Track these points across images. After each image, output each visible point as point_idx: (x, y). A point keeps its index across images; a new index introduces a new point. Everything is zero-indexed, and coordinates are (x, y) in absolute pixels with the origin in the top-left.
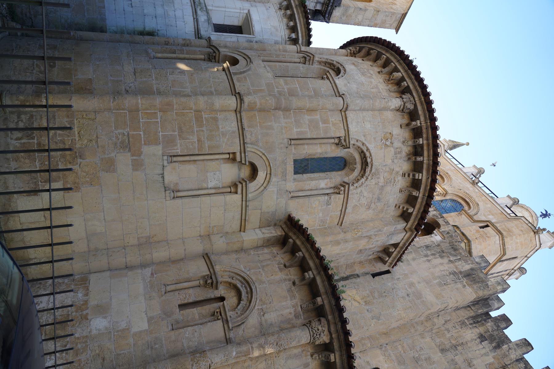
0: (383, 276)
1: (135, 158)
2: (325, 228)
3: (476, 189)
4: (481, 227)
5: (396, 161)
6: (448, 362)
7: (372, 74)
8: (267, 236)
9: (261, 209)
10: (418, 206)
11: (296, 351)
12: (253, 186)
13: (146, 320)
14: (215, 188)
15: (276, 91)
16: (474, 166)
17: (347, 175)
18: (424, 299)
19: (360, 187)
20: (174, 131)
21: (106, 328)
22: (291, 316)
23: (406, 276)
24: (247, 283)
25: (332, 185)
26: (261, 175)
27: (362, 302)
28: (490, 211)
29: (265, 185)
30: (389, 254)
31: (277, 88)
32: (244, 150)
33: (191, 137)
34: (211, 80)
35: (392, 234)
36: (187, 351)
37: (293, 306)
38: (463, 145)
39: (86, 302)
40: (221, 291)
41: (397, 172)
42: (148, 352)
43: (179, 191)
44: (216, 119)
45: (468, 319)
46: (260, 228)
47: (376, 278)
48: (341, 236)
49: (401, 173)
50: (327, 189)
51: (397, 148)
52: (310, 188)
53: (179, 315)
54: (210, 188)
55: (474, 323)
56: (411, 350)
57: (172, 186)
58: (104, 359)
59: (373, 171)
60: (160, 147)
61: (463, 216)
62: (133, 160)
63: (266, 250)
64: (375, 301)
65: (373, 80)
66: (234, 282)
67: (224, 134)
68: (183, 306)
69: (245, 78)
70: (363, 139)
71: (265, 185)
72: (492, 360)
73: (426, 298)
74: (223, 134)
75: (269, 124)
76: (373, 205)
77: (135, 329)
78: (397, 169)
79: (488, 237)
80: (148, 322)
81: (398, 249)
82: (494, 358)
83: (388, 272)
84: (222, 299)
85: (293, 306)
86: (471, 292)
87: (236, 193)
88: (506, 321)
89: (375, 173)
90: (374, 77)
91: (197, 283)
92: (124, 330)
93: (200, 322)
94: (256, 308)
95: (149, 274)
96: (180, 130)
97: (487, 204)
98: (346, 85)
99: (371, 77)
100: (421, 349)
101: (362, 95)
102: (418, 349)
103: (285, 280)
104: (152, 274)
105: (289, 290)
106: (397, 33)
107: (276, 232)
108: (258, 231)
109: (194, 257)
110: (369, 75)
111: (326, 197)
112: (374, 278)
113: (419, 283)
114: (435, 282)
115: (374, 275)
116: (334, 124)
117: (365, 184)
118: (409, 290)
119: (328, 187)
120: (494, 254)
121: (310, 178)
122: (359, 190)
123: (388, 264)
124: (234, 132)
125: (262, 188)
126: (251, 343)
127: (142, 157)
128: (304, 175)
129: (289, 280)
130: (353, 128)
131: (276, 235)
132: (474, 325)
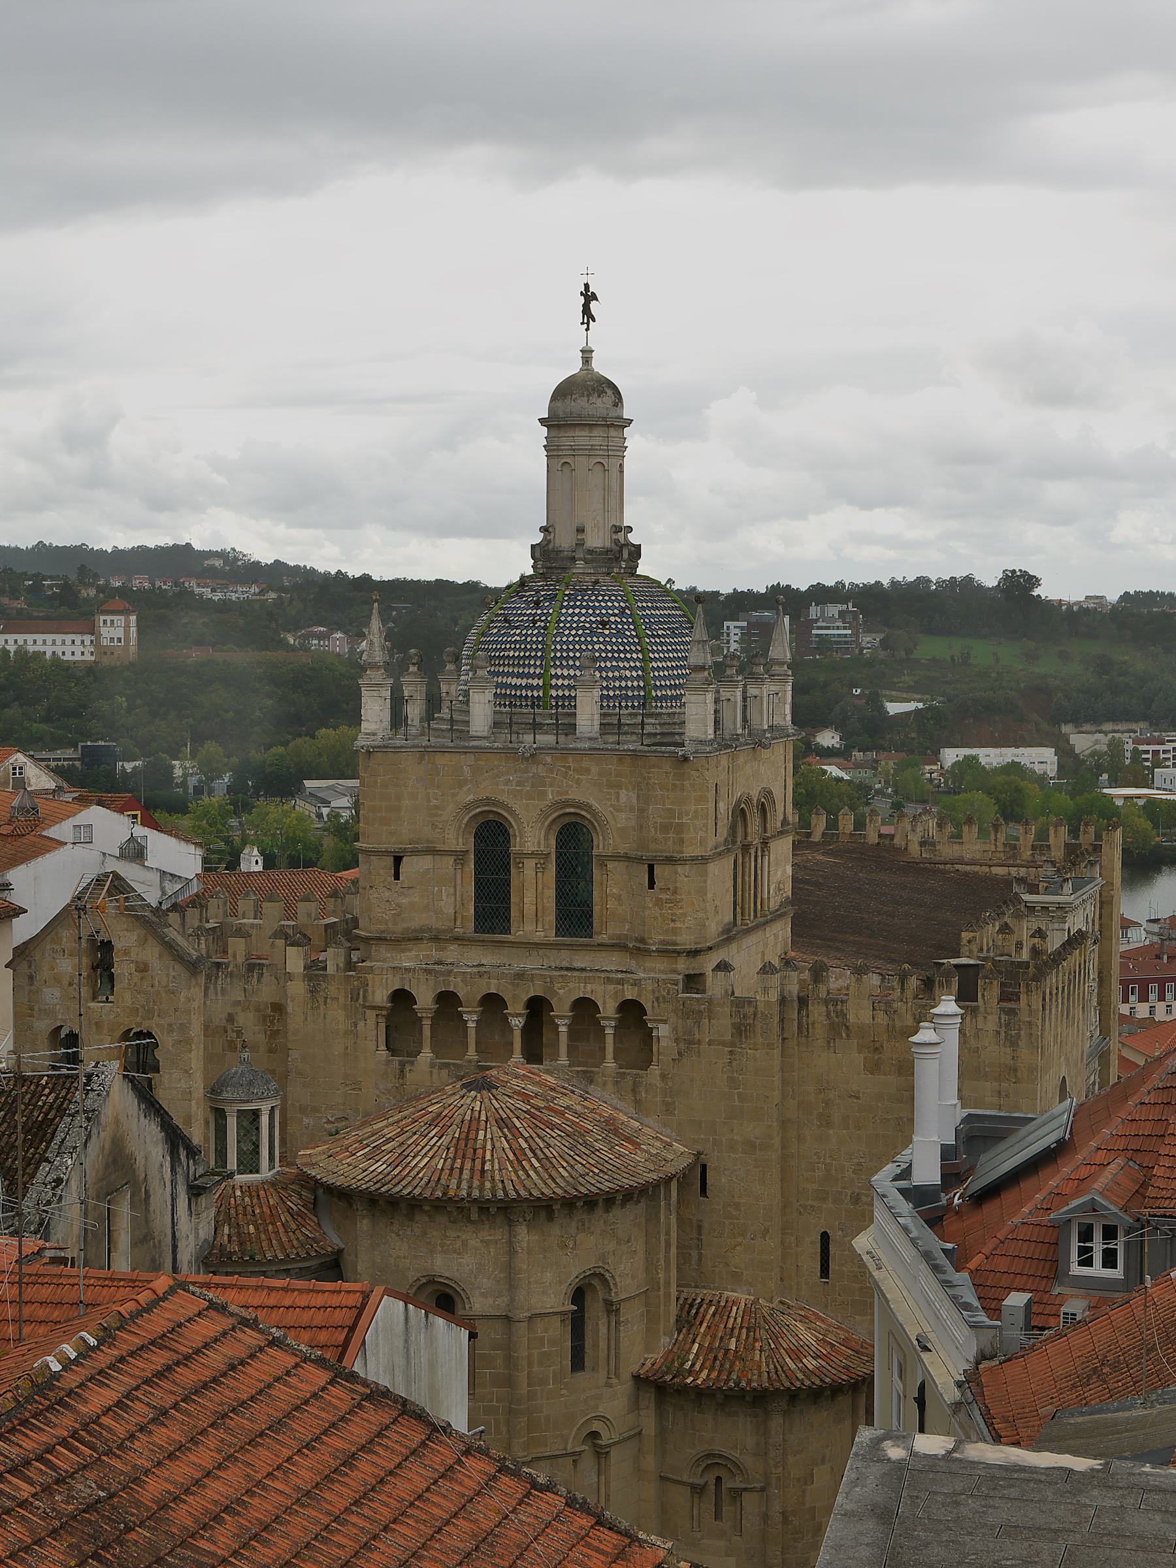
3: (542, 756)
4: (651, 884)
7: (458, 1237)
8: (652, 1405)
26: (596, 1426)
31: (492, 1401)
32: (573, 1454)
40: (711, 1478)
45: (799, 1044)
48: (661, 1293)
50: (609, 1322)
52: (606, 1347)
55: (807, 1037)
61: (610, 865)
66: (704, 1465)
68: (718, 1516)
70: (564, 1287)
73: (757, 1138)
86: (767, 1054)
93: (739, 1509)
94: (738, 1456)
97: (588, 771)
99: (465, 1243)
101: (502, 1275)
110: (459, 1243)
111: (622, 1328)
125: (607, 1422)
128: (587, 1351)
129: (717, 1410)
131: (653, 1395)
132: (810, 1039)
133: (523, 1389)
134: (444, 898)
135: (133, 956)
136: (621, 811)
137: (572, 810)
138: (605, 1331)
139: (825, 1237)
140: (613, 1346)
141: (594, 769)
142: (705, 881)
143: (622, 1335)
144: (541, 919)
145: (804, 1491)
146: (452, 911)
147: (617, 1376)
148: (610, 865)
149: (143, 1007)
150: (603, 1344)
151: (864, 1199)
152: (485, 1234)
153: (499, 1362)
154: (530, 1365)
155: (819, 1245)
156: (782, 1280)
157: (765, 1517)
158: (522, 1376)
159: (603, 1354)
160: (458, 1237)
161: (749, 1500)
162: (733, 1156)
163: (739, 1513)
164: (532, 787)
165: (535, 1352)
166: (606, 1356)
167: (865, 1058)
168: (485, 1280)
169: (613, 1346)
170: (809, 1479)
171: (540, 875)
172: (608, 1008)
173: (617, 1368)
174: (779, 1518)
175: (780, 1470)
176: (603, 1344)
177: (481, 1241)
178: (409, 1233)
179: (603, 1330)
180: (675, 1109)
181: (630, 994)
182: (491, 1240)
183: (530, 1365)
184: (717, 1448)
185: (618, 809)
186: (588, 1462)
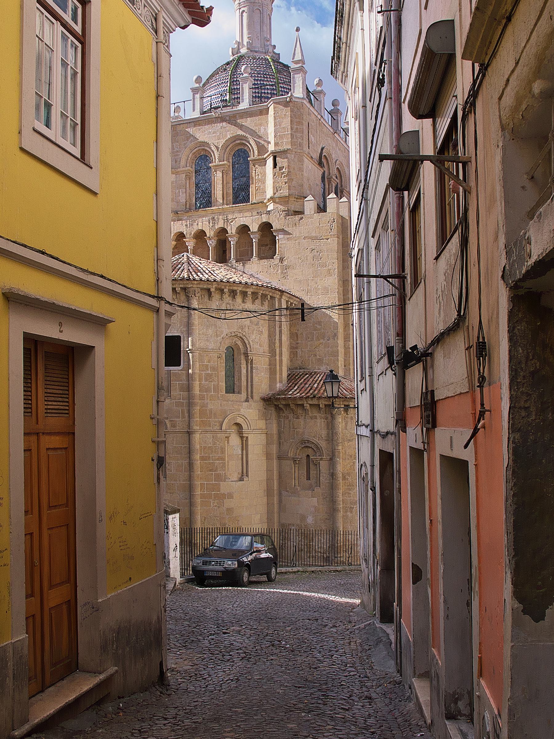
2: (270, 369)
9: (257, 420)
12: (244, 426)
14: (242, 450)
15: (183, 401)
17: (239, 349)
19: (249, 342)
21: (313, 517)
22: (326, 422)
24: (303, 442)
25: (245, 362)
26: (239, 421)
27: (322, 341)
29: (244, 418)
36: (331, 481)
42: (328, 499)
43: (242, 472)
48: (277, 358)
50: (247, 367)
53: (312, 481)
54: (242, 452)
59: (240, 331)
63: (282, 420)
67: (214, 443)
68: (308, 478)
71: (244, 418)
84: (308, 456)
87: (247, 437)
89: (242, 329)
91: (297, 468)
93: (318, 472)
96: (211, 470)
101: (185, 329)
103: (305, 418)
107: (272, 411)
109: (280, 466)
111: (254, 371)
112: (305, 321)
116: (209, 362)
117: (248, 337)
121: (239, 380)
122: (251, 342)
124: (213, 437)
125: (246, 420)
127: (226, 493)
130: (211, 346)
137: (239, 142)
138: (245, 372)
140: (249, 380)
142: (302, 164)
144: (225, 198)
147: (252, 398)
150: (244, 379)
156: (345, 366)
158: (196, 385)
159: (244, 383)
161: (324, 465)
163: (318, 473)
169: (249, 380)
172: (254, 228)
173: (252, 392)
176: (244, 379)
179: (244, 371)
184: (306, 437)
186: (235, 440)
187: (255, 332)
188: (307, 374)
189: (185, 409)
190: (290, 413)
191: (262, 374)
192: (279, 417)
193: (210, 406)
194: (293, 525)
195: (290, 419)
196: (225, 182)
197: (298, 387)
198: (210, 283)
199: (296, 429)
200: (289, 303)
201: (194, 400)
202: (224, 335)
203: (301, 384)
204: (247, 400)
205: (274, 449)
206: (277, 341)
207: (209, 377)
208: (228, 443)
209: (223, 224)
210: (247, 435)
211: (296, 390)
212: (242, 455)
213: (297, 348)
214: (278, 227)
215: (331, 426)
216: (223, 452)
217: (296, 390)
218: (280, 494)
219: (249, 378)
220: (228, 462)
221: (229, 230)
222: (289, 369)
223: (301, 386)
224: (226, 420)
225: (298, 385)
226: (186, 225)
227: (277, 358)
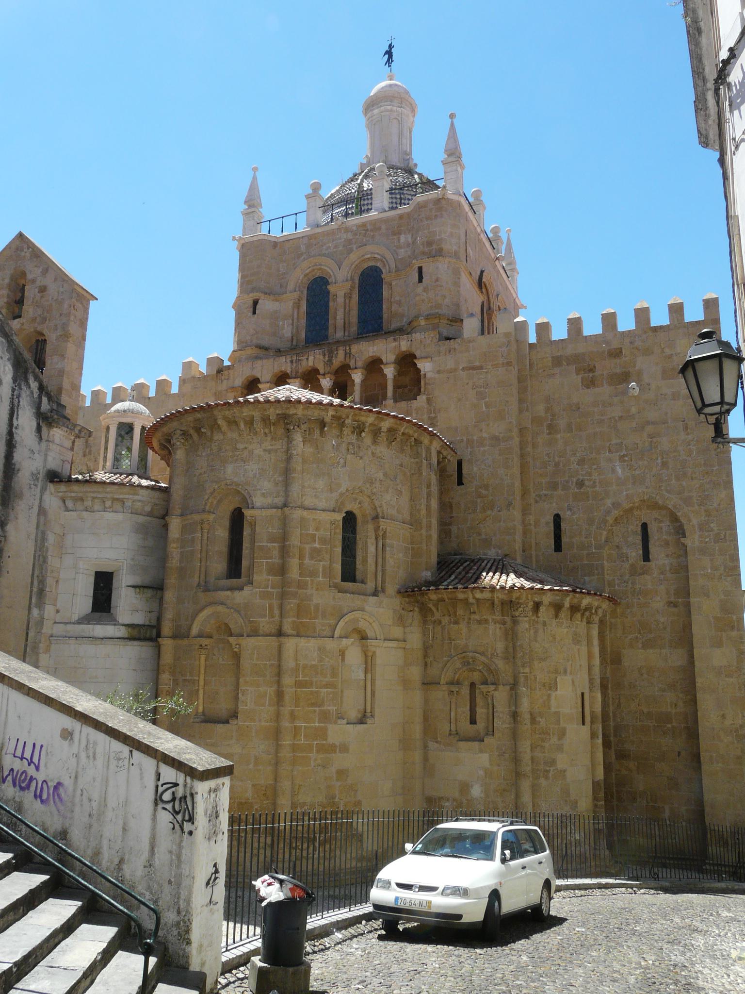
0: (463, 472)
1: (338, 750)
2: (413, 549)
4: (420, 279)
5: (361, 454)
6: (569, 432)
7: (246, 448)
10: (411, 432)
11: (532, 632)
13: (480, 755)
14: (366, 673)
16: (308, 197)
18: (501, 435)
20: (315, 711)
23: (468, 440)
27: (489, 512)
28: (394, 234)
30: (444, 458)
31: (267, 587)
33: (322, 694)
34: (255, 662)
35: (430, 465)
36: (512, 725)
37: (495, 623)
38: (255, 178)
39: (454, 800)
41: (373, 453)
42: (507, 755)
44: (305, 667)
46: (404, 627)
47: (464, 481)
49: (373, 447)
51: (348, 450)
53: (481, 725)
56: (546, 468)
57: (360, 716)
58: (504, 790)
60: (330, 727)
62: (340, 752)
64: (490, 498)
65: (256, 452)
68: (473, 721)
69: (251, 622)
70: (335, 495)
72: (580, 376)
73: (500, 433)
74: (321, 661)
75: (312, 608)
76: (399, 487)
77: (487, 764)
78: (370, 453)
79: (437, 280)
80: (482, 752)
81: (442, 451)
82: (577, 374)
83: (460, 464)
85: (495, 623)
88: (543, 329)
90: (250, 447)
92: (486, 773)
95: (436, 745)
96: (313, 705)
97: (380, 228)
98: (263, 494)
100: (548, 455)
101: (280, 479)
102: (546, 458)
103: (468, 623)
104: (437, 742)
105: (480, 622)
106: (97, 299)
108: (408, 630)
109: (426, 701)
110: (246, 453)
113: (481, 431)
114: (484, 409)
115: (460, 482)
118: (486, 448)
119: (374, 542)
120: (459, 278)
121: (363, 562)
123: (451, 459)
126: (519, 673)
127: (338, 744)
133: (294, 573)
134: (286, 326)
135: (38, 283)
136: (401, 248)
137: (369, 256)
139: (557, 519)
140: (380, 564)
141: (383, 227)
143: (388, 556)
145: (549, 696)
146: (290, 335)
148: (394, 283)
149: (40, 315)
150: (371, 560)
151: (587, 483)
152: (267, 445)
153: (276, 553)
154: (301, 557)
155: (552, 525)
156: (524, 551)
157: (515, 715)
158: (294, 563)
159: (371, 567)
160: (246, 448)
162: (482, 449)
164: (344, 246)
165: (307, 546)
166: (374, 572)
167: (582, 378)
168: (266, 483)
169: (380, 564)
170: (553, 686)
171: (347, 301)
174: (527, 716)
175: (527, 670)
176: (371, 560)
177: (265, 450)
178: (209, 452)
179: (372, 549)
180: (437, 422)
181: (404, 345)
182: (272, 450)
183: (301, 557)
185: (399, 247)
187: (390, 491)
188: (466, 561)
189: (275, 603)
190: (444, 616)
191: (401, 555)
192: (425, 622)
193: (316, 600)
194: (448, 800)
195: (443, 624)
196: (347, 309)
197: (456, 578)
198: (324, 408)
199: (454, 640)
200: (442, 456)
201: (289, 587)
202: (343, 489)
203: (460, 573)
204: (375, 594)
205: (415, 673)
206: (423, 507)
207: (316, 554)
208: (343, 660)
209: (343, 356)
210: (373, 649)
211: (453, 581)
212: (365, 680)
213: (450, 524)
214: (423, 355)
215: (511, 635)
216: (334, 674)
217: (453, 581)
218: (425, 747)
219: (380, 560)
220: (342, 692)
221: (352, 364)
222: (439, 555)
223: (460, 576)
224: (342, 623)
225: (456, 574)
226: (292, 362)
227: (424, 532)
